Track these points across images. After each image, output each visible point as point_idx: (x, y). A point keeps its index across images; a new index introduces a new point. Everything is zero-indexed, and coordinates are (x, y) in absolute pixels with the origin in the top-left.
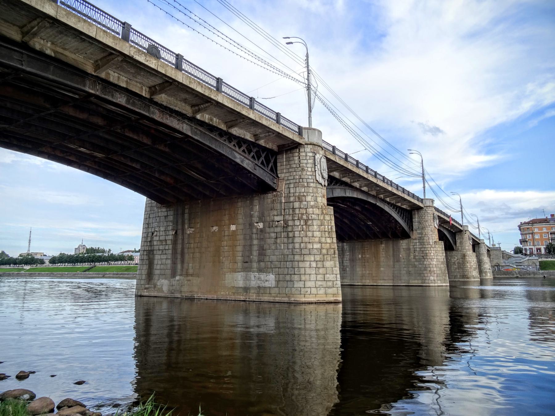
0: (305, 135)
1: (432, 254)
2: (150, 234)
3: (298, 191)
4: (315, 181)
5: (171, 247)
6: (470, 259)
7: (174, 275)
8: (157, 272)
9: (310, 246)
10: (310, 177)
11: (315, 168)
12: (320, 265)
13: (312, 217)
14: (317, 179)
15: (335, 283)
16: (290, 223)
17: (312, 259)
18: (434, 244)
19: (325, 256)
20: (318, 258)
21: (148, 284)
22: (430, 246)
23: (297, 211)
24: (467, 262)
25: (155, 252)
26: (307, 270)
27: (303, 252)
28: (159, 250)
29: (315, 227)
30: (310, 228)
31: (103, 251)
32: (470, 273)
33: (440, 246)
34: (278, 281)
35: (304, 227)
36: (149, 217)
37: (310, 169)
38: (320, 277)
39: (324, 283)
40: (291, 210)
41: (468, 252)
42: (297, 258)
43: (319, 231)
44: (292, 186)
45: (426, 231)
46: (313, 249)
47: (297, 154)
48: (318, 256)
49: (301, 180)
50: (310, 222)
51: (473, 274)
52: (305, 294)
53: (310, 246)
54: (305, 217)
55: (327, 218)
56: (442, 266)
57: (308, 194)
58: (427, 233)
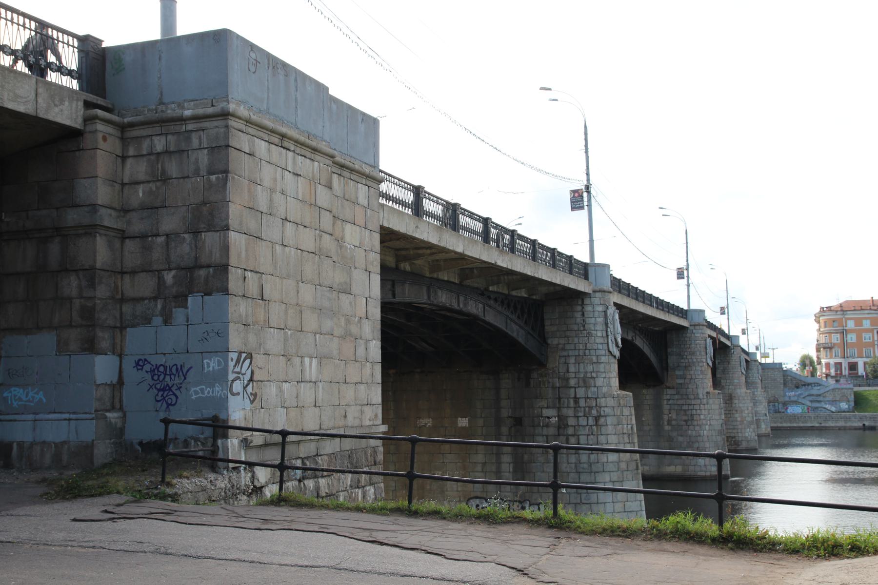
1: (702, 417)
3: (582, 370)
4: (607, 353)
6: (741, 405)
10: (600, 347)
13: (604, 411)
14: (611, 349)
16: (571, 421)
18: (705, 397)
19: (625, 473)
22: (698, 401)
23: (582, 403)
24: (736, 411)
27: (594, 468)
29: (610, 428)
30: (603, 429)
32: (741, 433)
33: (717, 401)
35: (594, 427)
37: (599, 334)
40: (572, 401)
41: (738, 391)
43: (615, 434)
44: (572, 360)
45: (692, 372)
46: (607, 462)
48: (615, 474)
49: (587, 351)
50: (602, 420)
51: (747, 435)
54: (594, 412)
56: (719, 438)
57: (599, 374)
58: (694, 377)
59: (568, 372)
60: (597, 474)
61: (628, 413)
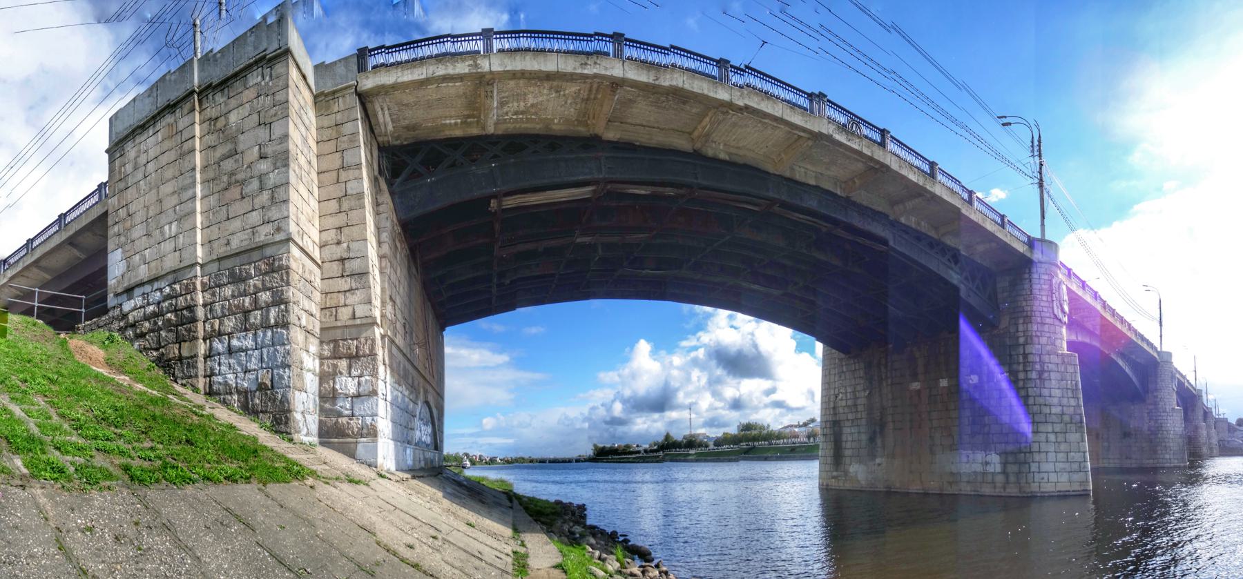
2: (832, 398)
4: (1052, 316)
5: (864, 415)
7: (873, 456)
8: (847, 453)
11: (1052, 297)
12: (1061, 438)
14: (1056, 312)
15: (1082, 465)
17: (1050, 429)
19: (1069, 426)
20: (1058, 428)
21: (837, 471)
25: (842, 425)
26: (1043, 446)
28: (848, 420)
30: (1047, 384)
31: (762, 428)
34: (1005, 464)
35: (1038, 381)
36: (830, 374)
37: (1044, 298)
38: (1061, 456)
39: (1067, 466)
43: (1059, 388)
44: (1021, 321)
46: (1050, 414)
47: (1027, 276)
48: (1058, 425)
50: (1046, 375)
52: (1040, 483)
53: (1046, 410)
55: (1071, 369)
57: (1043, 333)
59: (1018, 331)
60: (1039, 424)
61: (1072, 370)
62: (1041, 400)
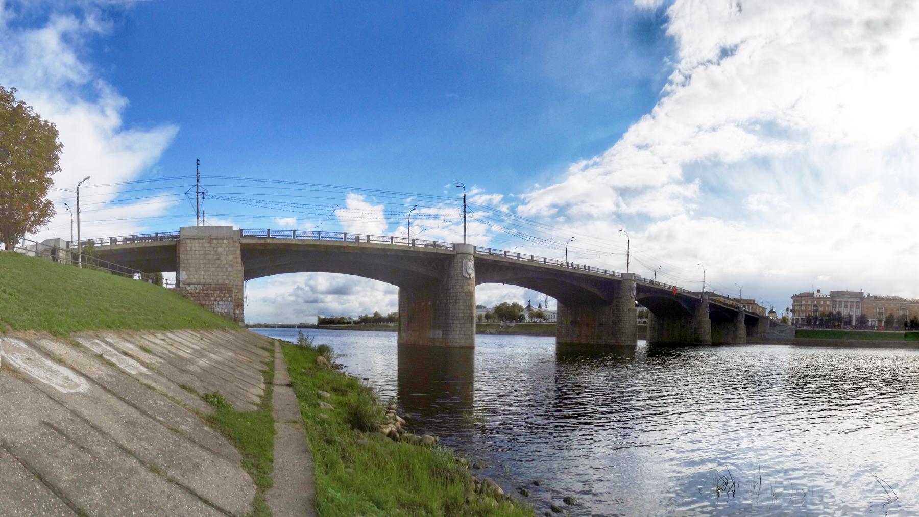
0: (457, 249)
9: (457, 315)
12: (463, 326)
20: (461, 322)
23: (452, 294)
30: (458, 304)
39: (464, 337)
42: (451, 321)
50: (458, 301)
53: (457, 315)
54: (455, 298)
62: (455, 311)
